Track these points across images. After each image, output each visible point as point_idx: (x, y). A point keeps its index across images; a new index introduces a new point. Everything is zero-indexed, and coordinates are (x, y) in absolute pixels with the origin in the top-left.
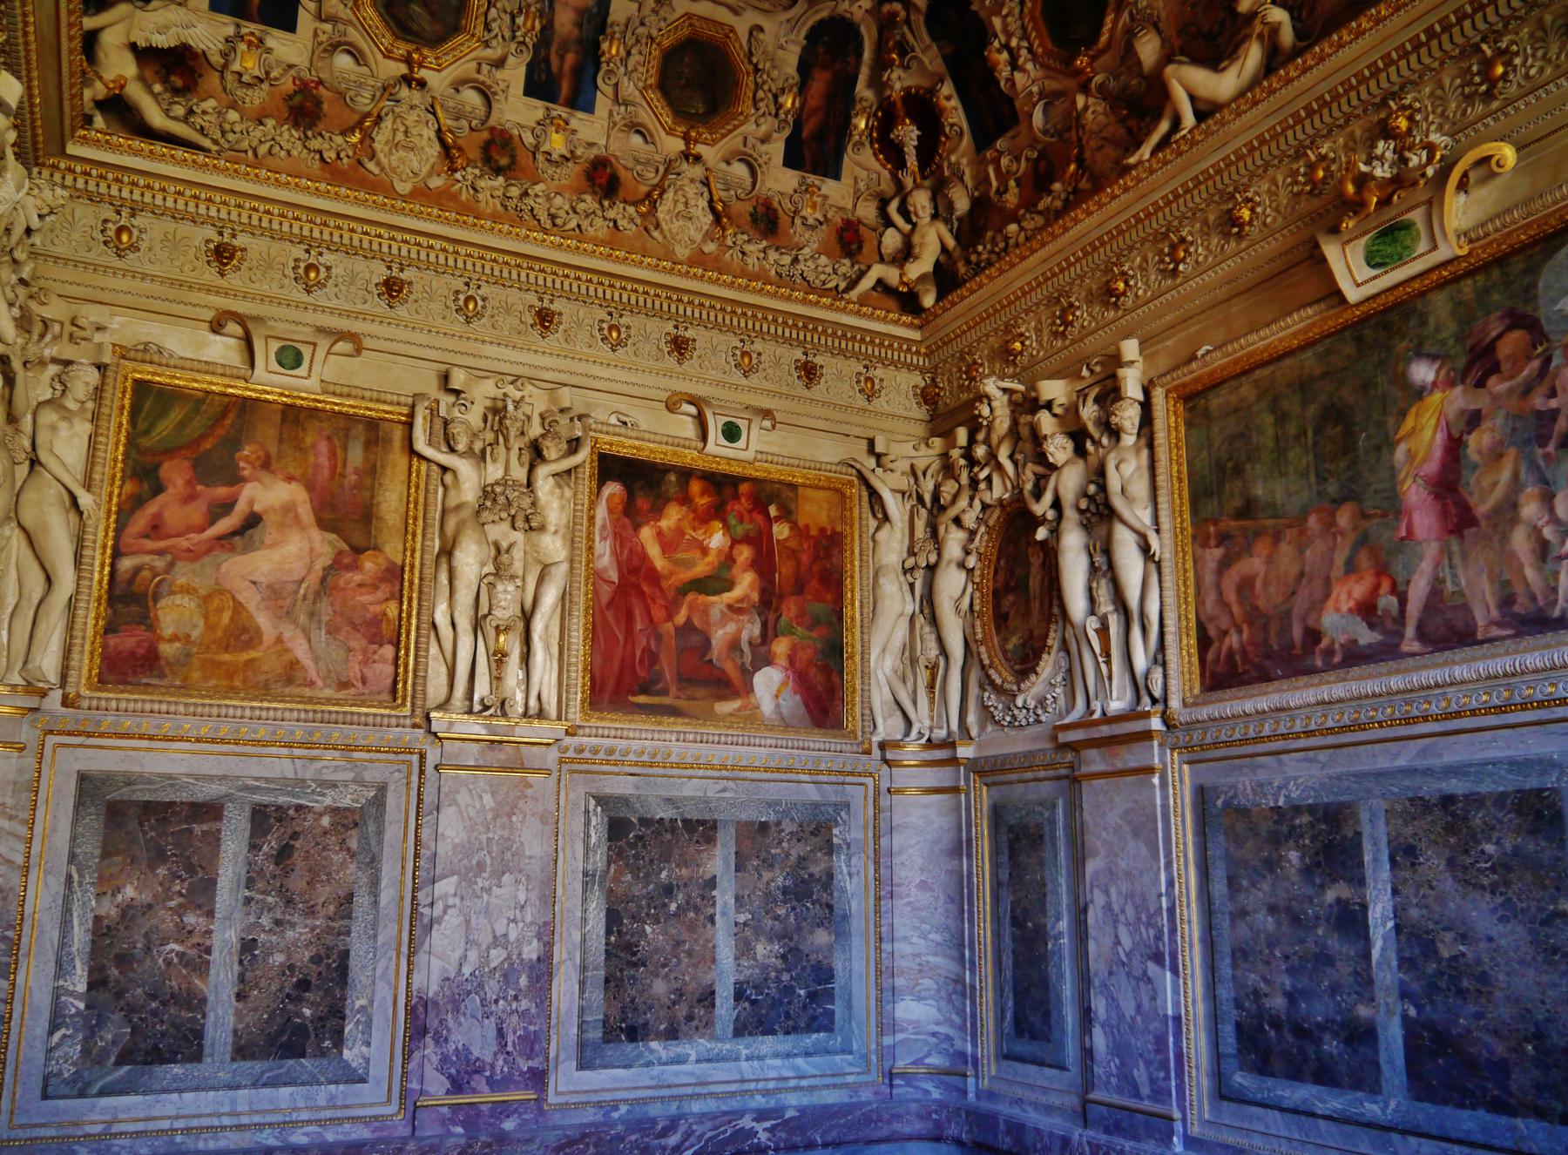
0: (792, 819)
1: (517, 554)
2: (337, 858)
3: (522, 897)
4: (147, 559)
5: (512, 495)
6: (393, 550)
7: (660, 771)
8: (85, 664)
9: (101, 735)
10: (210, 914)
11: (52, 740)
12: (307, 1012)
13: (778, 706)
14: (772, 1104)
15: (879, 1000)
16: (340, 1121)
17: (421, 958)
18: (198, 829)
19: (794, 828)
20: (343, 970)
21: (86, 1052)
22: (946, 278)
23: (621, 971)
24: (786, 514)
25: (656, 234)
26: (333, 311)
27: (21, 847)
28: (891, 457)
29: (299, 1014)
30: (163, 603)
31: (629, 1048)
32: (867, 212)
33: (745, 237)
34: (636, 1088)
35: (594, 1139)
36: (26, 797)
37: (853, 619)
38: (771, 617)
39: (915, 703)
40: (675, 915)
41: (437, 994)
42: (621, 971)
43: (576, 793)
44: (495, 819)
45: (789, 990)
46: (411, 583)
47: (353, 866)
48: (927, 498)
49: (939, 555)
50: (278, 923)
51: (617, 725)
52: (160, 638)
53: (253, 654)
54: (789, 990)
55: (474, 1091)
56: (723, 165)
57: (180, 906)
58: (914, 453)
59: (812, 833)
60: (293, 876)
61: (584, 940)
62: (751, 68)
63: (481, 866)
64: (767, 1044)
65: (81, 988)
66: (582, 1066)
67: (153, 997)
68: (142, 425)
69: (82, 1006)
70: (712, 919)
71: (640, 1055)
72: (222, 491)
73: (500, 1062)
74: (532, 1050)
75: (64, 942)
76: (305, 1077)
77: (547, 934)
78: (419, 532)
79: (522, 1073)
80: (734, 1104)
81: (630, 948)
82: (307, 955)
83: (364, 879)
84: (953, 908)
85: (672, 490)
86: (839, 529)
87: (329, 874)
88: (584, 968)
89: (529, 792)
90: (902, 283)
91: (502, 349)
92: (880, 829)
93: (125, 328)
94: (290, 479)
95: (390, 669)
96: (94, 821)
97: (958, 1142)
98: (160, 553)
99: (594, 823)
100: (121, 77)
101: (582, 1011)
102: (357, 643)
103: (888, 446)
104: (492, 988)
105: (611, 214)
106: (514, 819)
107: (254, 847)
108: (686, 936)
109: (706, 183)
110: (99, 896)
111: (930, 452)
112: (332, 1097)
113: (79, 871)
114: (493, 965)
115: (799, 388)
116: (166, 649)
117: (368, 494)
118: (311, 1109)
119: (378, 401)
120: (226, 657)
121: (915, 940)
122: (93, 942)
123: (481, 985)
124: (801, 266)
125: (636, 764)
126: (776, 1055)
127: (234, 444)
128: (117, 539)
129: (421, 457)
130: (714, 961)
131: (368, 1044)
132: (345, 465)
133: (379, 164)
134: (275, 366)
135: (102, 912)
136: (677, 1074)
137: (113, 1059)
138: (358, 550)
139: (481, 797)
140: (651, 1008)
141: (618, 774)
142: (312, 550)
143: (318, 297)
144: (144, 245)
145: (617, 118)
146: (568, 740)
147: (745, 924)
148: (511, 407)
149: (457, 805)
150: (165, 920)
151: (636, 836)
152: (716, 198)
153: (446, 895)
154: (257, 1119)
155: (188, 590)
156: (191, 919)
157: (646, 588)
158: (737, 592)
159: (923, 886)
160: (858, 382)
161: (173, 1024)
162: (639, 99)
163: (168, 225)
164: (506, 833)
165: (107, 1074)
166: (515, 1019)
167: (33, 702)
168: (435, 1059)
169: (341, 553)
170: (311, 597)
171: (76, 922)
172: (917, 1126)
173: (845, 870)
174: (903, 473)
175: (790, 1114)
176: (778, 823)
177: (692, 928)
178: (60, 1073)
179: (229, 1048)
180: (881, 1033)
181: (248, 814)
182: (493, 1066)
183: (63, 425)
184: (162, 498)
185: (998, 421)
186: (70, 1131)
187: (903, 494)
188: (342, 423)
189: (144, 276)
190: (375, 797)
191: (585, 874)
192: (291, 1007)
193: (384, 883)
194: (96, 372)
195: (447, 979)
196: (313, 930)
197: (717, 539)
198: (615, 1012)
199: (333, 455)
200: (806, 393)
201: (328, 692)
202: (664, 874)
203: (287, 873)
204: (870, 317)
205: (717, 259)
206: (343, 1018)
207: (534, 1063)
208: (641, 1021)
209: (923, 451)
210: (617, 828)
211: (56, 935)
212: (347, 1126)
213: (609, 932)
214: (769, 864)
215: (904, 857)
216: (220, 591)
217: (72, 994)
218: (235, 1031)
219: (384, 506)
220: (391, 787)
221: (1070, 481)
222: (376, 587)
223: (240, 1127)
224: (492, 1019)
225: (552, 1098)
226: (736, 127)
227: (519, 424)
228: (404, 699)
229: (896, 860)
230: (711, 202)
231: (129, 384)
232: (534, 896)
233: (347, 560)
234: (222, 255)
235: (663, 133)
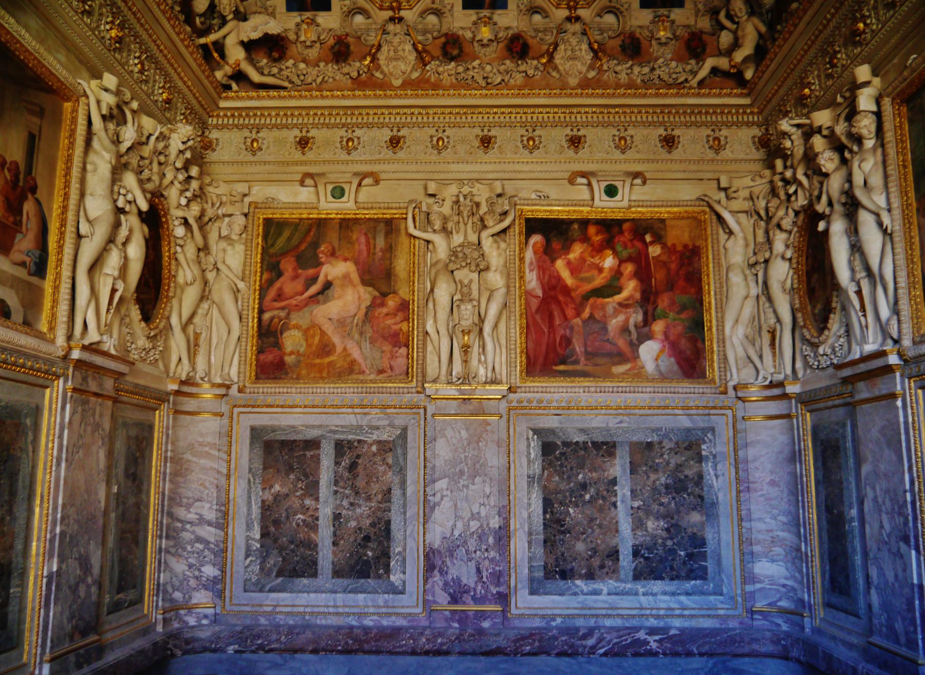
0: (671, 440)
1: (475, 287)
2: (382, 469)
3: (488, 491)
4: (276, 312)
5: (467, 251)
6: (404, 292)
7: (575, 412)
8: (250, 371)
9: (258, 406)
10: (317, 499)
11: (236, 410)
12: (370, 553)
13: (657, 366)
14: (662, 624)
15: (742, 561)
16: (389, 615)
17: (430, 525)
18: (309, 454)
19: (672, 445)
20: (388, 531)
21: (262, 569)
22: (760, 54)
23: (554, 536)
24: (658, 239)
25: (554, 74)
26: (361, 162)
27: (225, 465)
28: (733, 189)
29: (366, 555)
30: (285, 335)
31: (561, 583)
32: (705, 23)
33: (615, 62)
34: (568, 608)
35: (538, 637)
36: (225, 439)
37: (710, 303)
38: (650, 308)
39: (761, 357)
40: (589, 502)
41: (440, 546)
42: (554, 536)
43: (522, 428)
44: (469, 444)
45: (672, 551)
46: (413, 310)
47: (390, 473)
48: (763, 213)
49: (771, 252)
50: (352, 504)
51: (544, 385)
52: (285, 354)
53: (331, 358)
54: (672, 551)
55: (464, 603)
56: (598, 19)
57: (302, 495)
58: (752, 184)
59: (686, 449)
60: (358, 479)
61: (529, 517)
63: (462, 473)
64: (657, 586)
65: (258, 536)
66: (532, 593)
67: (292, 542)
68: (270, 242)
69: (259, 546)
70: (615, 505)
71: (569, 588)
72: (311, 272)
73: (479, 588)
74: (499, 581)
75: (249, 514)
76: (370, 589)
77: (505, 513)
78: (416, 280)
79: (493, 595)
80: (634, 623)
81: (559, 522)
82: (368, 522)
83: (397, 480)
84: (792, 498)
85: (576, 234)
86: (698, 243)
87: (377, 478)
88: (530, 534)
89: (489, 428)
90: (732, 67)
91: (460, 165)
92: (738, 443)
93: (259, 193)
94: (346, 260)
95: (405, 360)
96: (259, 451)
97: (798, 661)
98: (283, 308)
99: (532, 445)
100: (237, 60)
101: (530, 559)
102: (387, 347)
103: (730, 182)
104: (472, 544)
105: (522, 68)
106: (480, 444)
107: (337, 463)
108: (597, 515)
109: (584, 33)
110: (263, 489)
111: (764, 181)
112: (386, 601)
113: (253, 476)
114: (472, 530)
115: (663, 153)
116: (289, 359)
117: (388, 262)
118: (373, 606)
119: (388, 208)
120: (318, 361)
121: (768, 520)
122: (262, 513)
123: (465, 542)
124: (657, 72)
125: (558, 408)
126: (665, 593)
127: (315, 245)
128: (260, 304)
129: (415, 237)
130: (617, 531)
131: (404, 573)
132: (375, 248)
133: (382, 72)
134: (330, 198)
135: (265, 498)
136: (596, 601)
137: (274, 574)
138: (384, 295)
139: (460, 432)
140: (575, 559)
141: (547, 415)
142: (359, 298)
143: (355, 156)
144: (264, 147)
146: (512, 396)
147: (638, 508)
148: (462, 199)
149: (446, 437)
150: (295, 503)
151: (560, 453)
152: (592, 41)
153: (442, 489)
154: (347, 610)
155: (297, 327)
156: (308, 502)
157: (561, 298)
158: (625, 294)
159: (773, 483)
160: (708, 141)
161: (302, 557)
163: (276, 133)
164: (476, 453)
165: (272, 581)
166: (487, 562)
167: (222, 391)
168: (441, 583)
169: (375, 298)
170: (360, 324)
171: (253, 503)
172: (770, 648)
173: (712, 472)
174: (745, 199)
175: (672, 632)
176: (660, 443)
177: (601, 510)
178: (250, 579)
179: (330, 571)
180: (745, 581)
181: (333, 445)
182: (475, 590)
183: (229, 248)
184: (282, 279)
185: (796, 149)
186: (257, 609)
187: (746, 212)
188: (372, 224)
189: (265, 163)
190: (401, 434)
191: (529, 477)
192: (361, 551)
193: (408, 483)
194: (243, 218)
195: (445, 538)
196: (370, 508)
197: (609, 262)
198: (551, 561)
199: (368, 244)
200: (668, 156)
201: (372, 377)
202: (580, 476)
203: (355, 476)
204: (708, 95)
205: (598, 81)
206: (389, 558)
207: (501, 589)
208: (569, 567)
209: (759, 181)
210: (547, 449)
211: (245, 510)
212: (393, 618)
213: (545, 512)
214: (655, 469)
215: (757, 464)
216: (313, 325)
217: (254, 539)
218: (333, 563)
219: (397, 268)
220: (410, 428)
221: (835, 184)
222: (395, 315)
223: (337, 614)
224: (473, 562)
225: (514, 611)
227: (469, 208)
228: (413, 377)
229: (751, 466)
230: (590, 45)
231: (261, 221)
232: (495, 490)
233: (378, 301)
234: (303, 143)
235: (554, 9)
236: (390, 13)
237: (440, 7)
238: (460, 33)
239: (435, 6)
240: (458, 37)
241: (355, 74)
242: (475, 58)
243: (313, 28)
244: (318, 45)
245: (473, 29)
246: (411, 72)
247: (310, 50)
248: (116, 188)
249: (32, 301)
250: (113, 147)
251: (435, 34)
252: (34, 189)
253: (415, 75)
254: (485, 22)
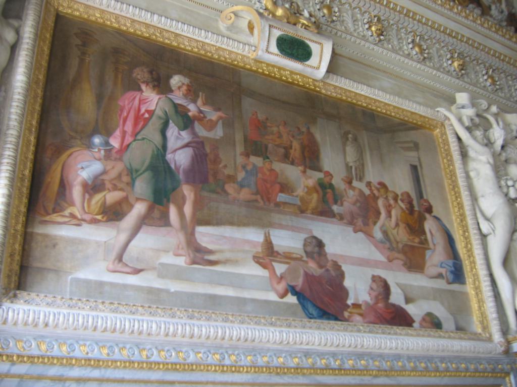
248: (503, 183)
249: (460, 306)
250: (485, 149)
252: (429, 210)
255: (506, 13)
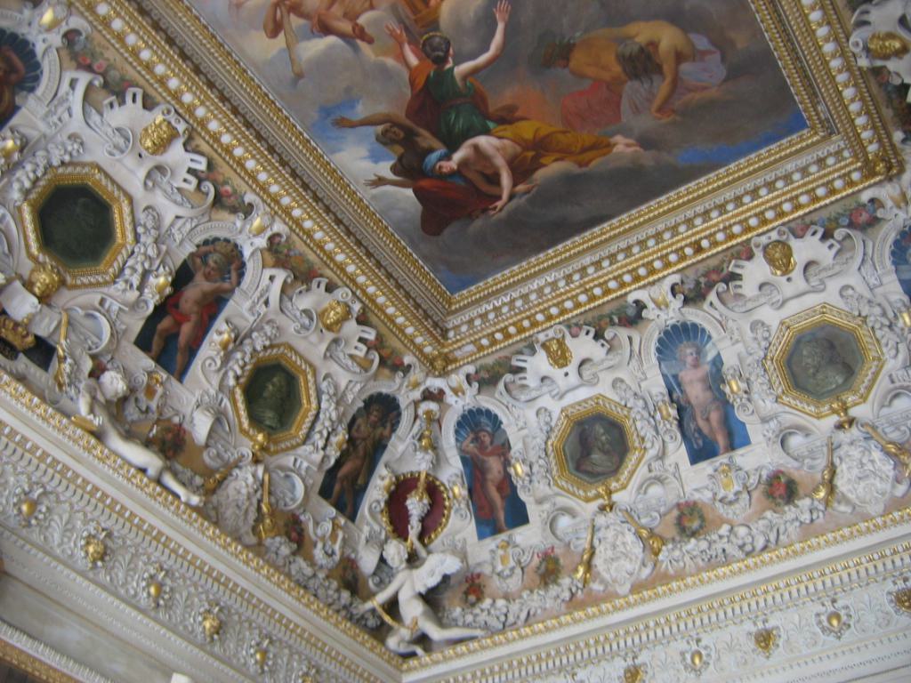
62: (859, 321)
145: (770, 435)
162: (778, 408)
226: (876, 375)
236: (600, 501)
237: (658, 474)
238: (697, 496)
239: (653, 474)
240: (695, 503)
241: (567, 595)
242: (723, 521)
243: (510, 550)
244: (518, 571)
245: (711, 486)
246: (640, 570)
247: (508, 581)
251: (662, 510)
253: (646, 572)
254: (723, 471)
255: (337, 558)
